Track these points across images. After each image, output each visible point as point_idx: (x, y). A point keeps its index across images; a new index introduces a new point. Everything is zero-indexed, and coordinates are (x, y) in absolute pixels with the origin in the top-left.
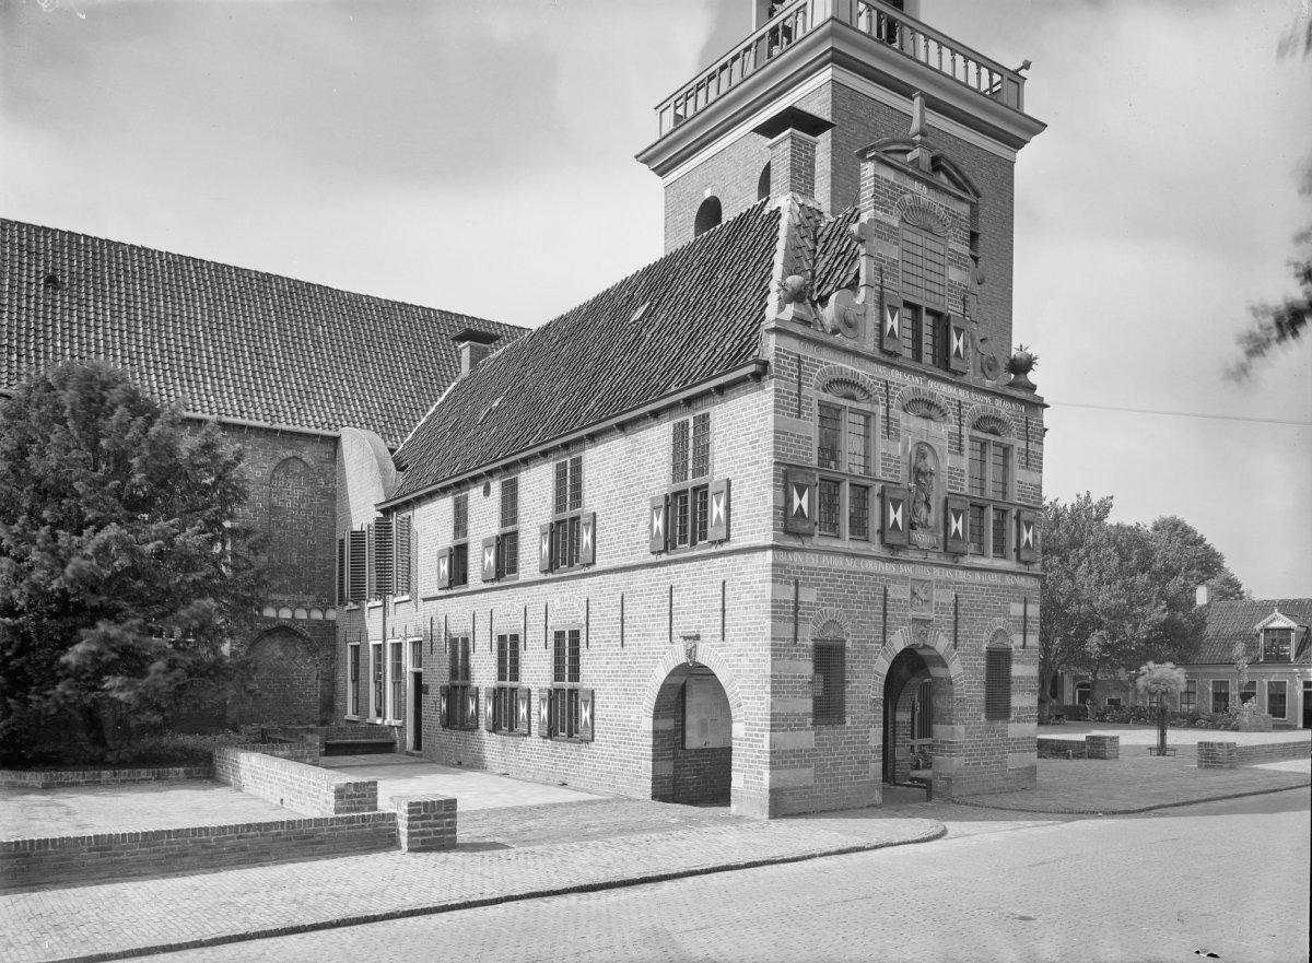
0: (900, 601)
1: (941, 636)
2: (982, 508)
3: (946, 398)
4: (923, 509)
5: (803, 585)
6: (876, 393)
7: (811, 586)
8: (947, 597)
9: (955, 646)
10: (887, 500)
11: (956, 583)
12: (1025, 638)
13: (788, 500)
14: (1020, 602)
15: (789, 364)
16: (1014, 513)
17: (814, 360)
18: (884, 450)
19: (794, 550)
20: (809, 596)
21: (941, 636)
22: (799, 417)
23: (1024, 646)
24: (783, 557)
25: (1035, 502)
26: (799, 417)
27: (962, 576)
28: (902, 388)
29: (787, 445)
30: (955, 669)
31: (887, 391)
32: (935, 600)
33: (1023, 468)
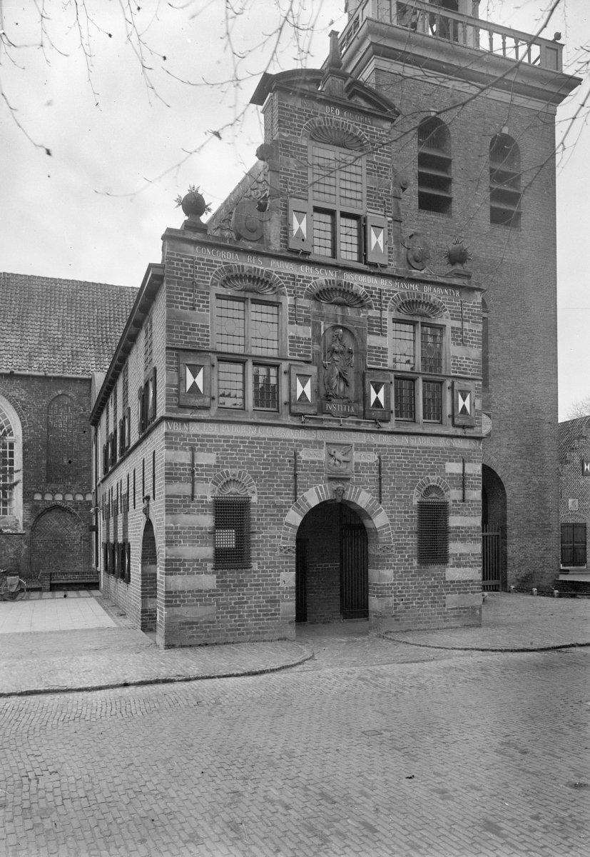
0: (313, 462)
1: (363, 492)
2: (413, 380)
3: (365, 287)
5: (201, 450)
6: (283, 286)
7: (209, 451)
10: (293, 375)
11: (379, 446)
12: (464, 495)
13: (182, 379)
15: (182, 265)
16: (448, 383)
17: (212, 261)
18: (291, 334)
19: (188, 421)
21: (363, 492)
22: (194, 309)
23: (463, 500)
25: (472, 374)
26: (194, 309)
27: (386, 440)
28: (313, 281)
29: (181, 332)
30: (380, 520)
32: (355, 460)
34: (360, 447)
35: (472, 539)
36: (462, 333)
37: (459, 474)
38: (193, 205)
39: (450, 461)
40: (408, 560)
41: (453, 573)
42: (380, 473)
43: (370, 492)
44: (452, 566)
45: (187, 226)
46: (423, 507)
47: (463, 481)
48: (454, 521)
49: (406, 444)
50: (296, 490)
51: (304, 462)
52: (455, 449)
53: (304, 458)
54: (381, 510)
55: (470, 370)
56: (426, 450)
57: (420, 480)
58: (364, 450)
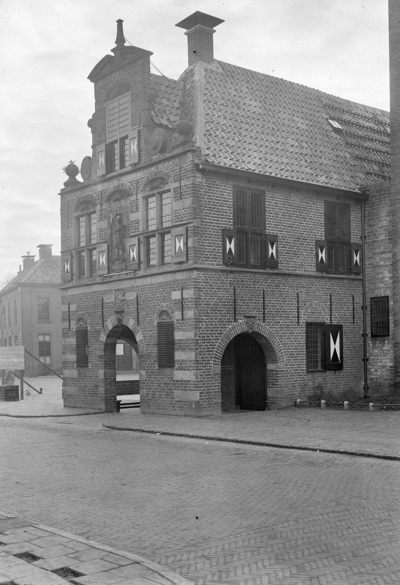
0: (109, 303)
11: (137, 287)
14: (178, 290)
20: (73, 308)
25: (187, 220)
27: (140, 282)
35: (190, 349)
38: (71, 170)
40: (152, 364)
41: (179, 375)
43: (133, 318)
44: (177, 370)
46: (160, 326)
47: (182, 304)
49: (150, 283)
52: (177, 281)
53: (106, 301)
55: (185, 217)
57: (158, 307)
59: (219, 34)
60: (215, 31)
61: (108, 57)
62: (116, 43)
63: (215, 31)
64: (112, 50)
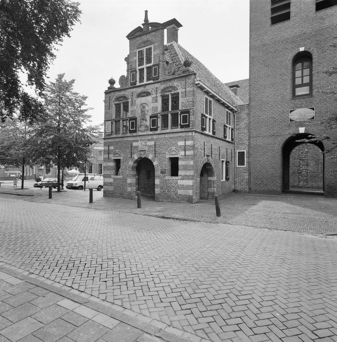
4: (144, 121)
5: (110, 146)
7: (112, 146)
8: (152, 143)
9: (155, 156)
20: (112, 148)
23: (185, 155)
24: (106, 141)
31: (132, 95)
33: (184, 98)
34: (149, 140)
36: (185, 93)
37: (183, 146)
38: (112, 82)
39: (180, 141)
42: (155, 148)
45: (109, 88)
48: (180, 163)
50: (131, 154)
51: (134, 146)
54: (155, 160)
56: (171, 138)
58: (150, 141)
59: (180, 30)
60: (179, 30)
61: (139, 27)
62: (144, 21)
63: (179, 30)
64: (143, 25)
